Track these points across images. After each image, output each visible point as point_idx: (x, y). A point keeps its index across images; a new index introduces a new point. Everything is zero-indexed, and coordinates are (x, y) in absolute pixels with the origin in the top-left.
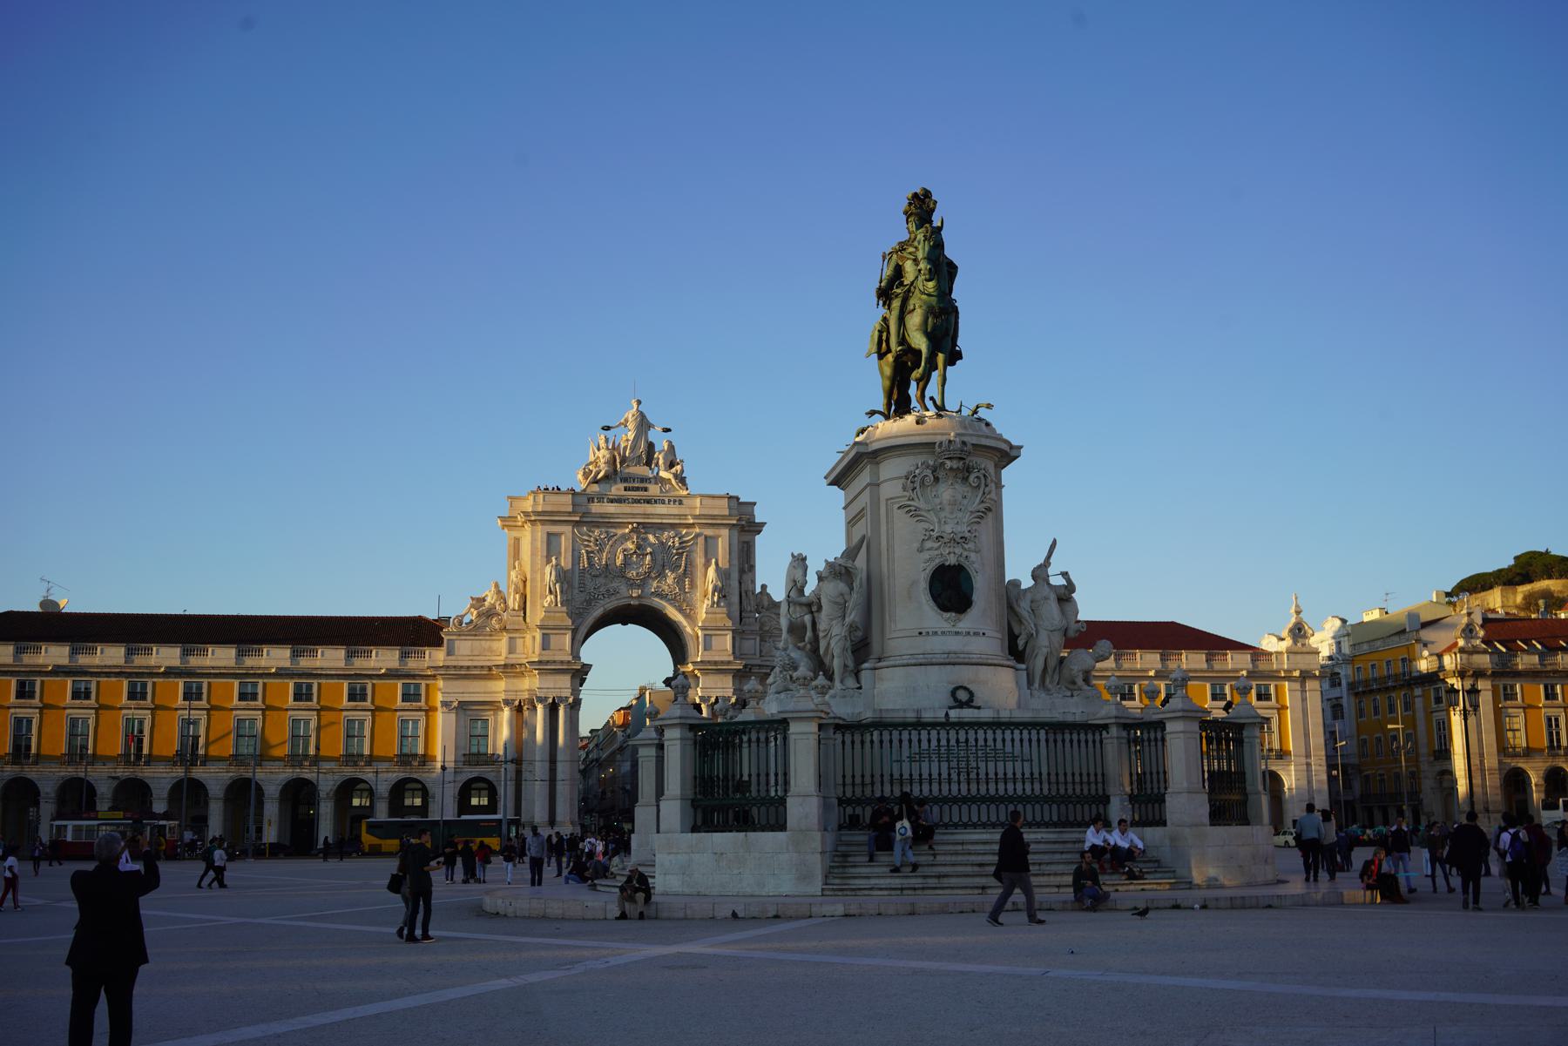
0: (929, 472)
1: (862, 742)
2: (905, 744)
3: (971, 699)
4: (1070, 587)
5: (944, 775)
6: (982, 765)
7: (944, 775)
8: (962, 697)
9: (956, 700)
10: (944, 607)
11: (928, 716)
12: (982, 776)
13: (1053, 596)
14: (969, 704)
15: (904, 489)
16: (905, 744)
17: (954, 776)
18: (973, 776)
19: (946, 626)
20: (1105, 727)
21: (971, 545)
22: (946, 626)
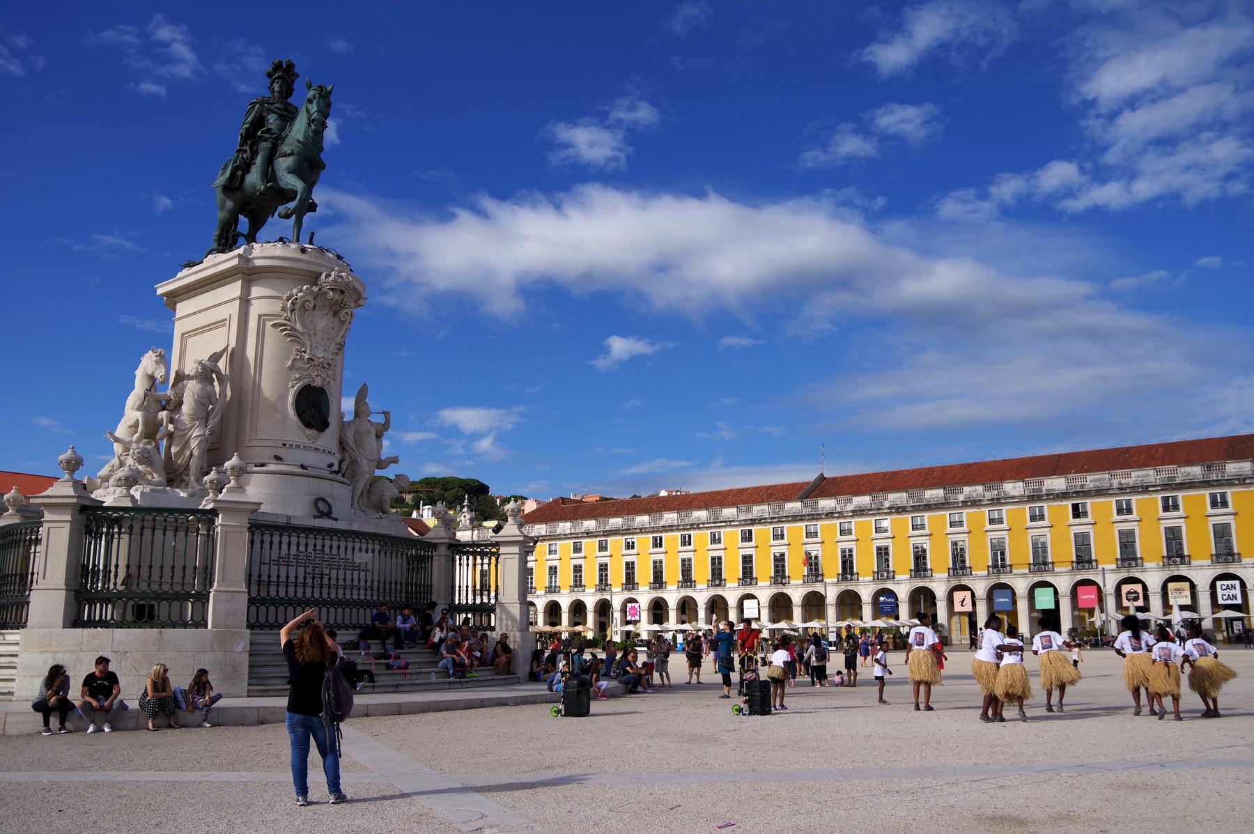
0: (311, 298)
1: (262, 542)
2: (276, 546)
3: (330, 512)
4: (386, 426)
5: (301, 580)
6: (334, 573)
7: (301, 580)
8: (322, 507)
9: (318, 510)
10: (308, 425)
11: (294, 522)
12: (333, 581)
13: (374, 431)
14: (328, 514)
15: (284, 309)
16: (276, 546)
17: (309, 581)
18: (325, 581)
19: (307, 442)
20: (434, 546)
21: (330, 372)
22: (307, 442)
